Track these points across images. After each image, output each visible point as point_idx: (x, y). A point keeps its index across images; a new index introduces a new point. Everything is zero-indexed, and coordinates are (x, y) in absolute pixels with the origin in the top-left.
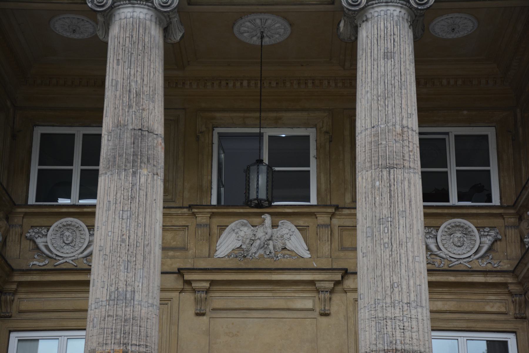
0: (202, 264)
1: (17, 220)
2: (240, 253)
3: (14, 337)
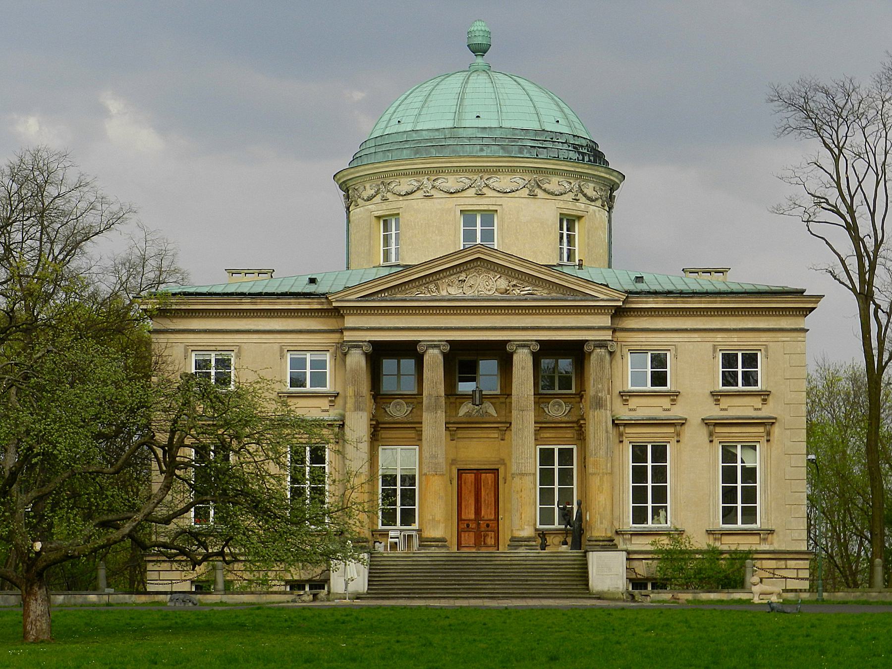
1: (378, 400)
2: (468, 414)
3: (380, 448)
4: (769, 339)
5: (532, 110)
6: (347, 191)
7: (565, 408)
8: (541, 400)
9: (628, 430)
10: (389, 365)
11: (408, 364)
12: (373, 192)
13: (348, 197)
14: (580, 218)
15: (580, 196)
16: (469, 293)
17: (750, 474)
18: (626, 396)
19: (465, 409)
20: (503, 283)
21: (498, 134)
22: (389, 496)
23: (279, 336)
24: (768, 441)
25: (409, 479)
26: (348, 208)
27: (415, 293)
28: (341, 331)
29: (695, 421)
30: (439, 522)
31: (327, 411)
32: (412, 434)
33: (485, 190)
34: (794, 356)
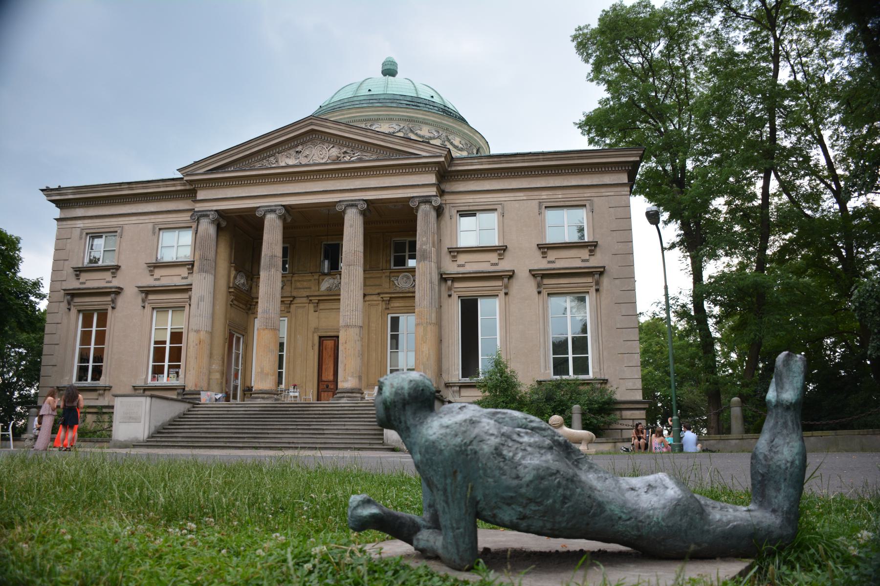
0: (316, 294)
4: (593, 194)
8: (392, 274)
9: (456, 285)
16: (304, 161)
20: (335, 152)
21: (382, 97)
23: (153, 217)
24: (597, 290)
27: (258, 165)
29: (523, 274)
30: (267, 374)
31: (186, 278)
34: (619, 209)
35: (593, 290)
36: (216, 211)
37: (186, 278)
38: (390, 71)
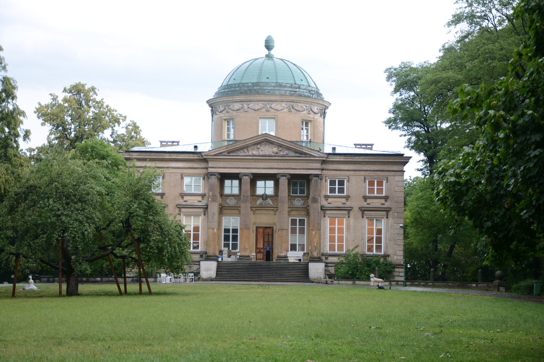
2: (261, 204)
3: (223, 217)
5: (291, 75)
6: (212, 108)
7: (302, 202)
9: (328, 212)
10: (227, 182)
11: (236, 183)
12: (222, 109)
13: (212, 110)
14: (310, 121)
15: (311, 112)
16: (261, 153)
17: (379, 231)
18: (327, 197)
19: (259, 201)
20: (275, 150)
22: (227, 238)
25: (235, 231)
26: (212, 115)
28: (207, 168)
29: (356, 209)
31: (201, 201)
32: (237, 212)
33: (270, 109)
35: (385, 217)
36: (219, 173)
37: (201, 201)
38: (269, 46)
